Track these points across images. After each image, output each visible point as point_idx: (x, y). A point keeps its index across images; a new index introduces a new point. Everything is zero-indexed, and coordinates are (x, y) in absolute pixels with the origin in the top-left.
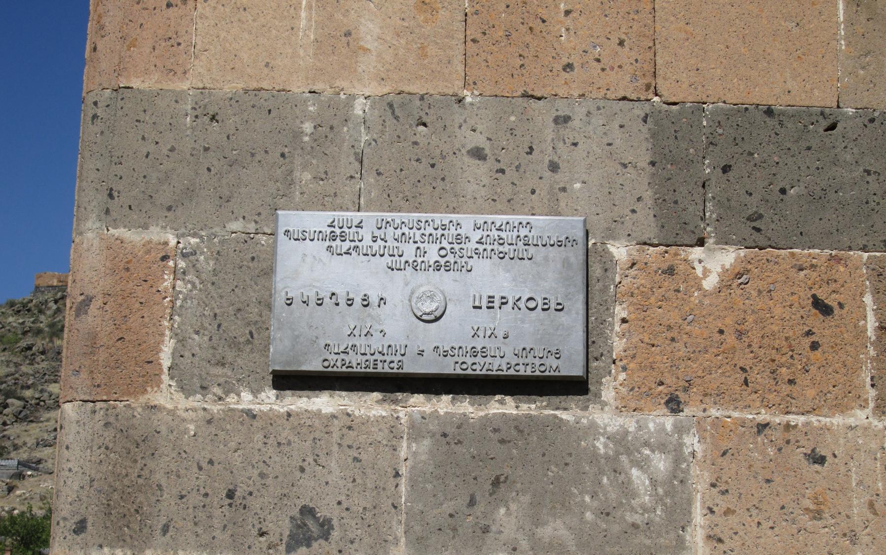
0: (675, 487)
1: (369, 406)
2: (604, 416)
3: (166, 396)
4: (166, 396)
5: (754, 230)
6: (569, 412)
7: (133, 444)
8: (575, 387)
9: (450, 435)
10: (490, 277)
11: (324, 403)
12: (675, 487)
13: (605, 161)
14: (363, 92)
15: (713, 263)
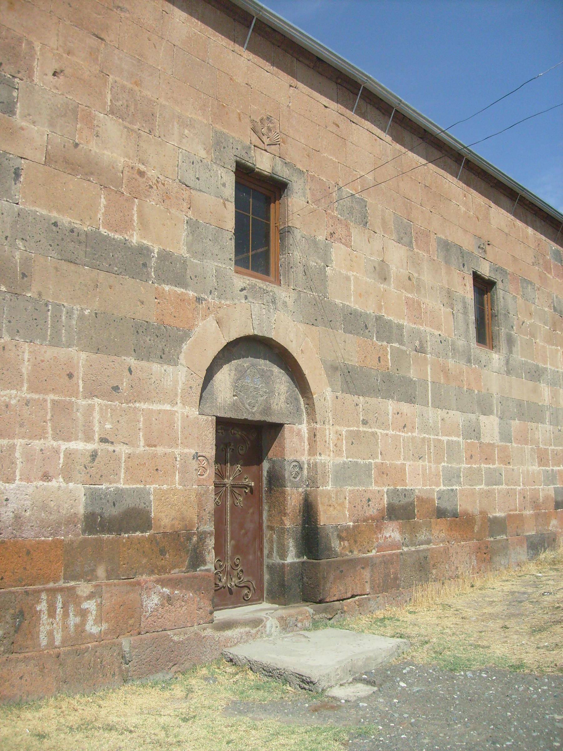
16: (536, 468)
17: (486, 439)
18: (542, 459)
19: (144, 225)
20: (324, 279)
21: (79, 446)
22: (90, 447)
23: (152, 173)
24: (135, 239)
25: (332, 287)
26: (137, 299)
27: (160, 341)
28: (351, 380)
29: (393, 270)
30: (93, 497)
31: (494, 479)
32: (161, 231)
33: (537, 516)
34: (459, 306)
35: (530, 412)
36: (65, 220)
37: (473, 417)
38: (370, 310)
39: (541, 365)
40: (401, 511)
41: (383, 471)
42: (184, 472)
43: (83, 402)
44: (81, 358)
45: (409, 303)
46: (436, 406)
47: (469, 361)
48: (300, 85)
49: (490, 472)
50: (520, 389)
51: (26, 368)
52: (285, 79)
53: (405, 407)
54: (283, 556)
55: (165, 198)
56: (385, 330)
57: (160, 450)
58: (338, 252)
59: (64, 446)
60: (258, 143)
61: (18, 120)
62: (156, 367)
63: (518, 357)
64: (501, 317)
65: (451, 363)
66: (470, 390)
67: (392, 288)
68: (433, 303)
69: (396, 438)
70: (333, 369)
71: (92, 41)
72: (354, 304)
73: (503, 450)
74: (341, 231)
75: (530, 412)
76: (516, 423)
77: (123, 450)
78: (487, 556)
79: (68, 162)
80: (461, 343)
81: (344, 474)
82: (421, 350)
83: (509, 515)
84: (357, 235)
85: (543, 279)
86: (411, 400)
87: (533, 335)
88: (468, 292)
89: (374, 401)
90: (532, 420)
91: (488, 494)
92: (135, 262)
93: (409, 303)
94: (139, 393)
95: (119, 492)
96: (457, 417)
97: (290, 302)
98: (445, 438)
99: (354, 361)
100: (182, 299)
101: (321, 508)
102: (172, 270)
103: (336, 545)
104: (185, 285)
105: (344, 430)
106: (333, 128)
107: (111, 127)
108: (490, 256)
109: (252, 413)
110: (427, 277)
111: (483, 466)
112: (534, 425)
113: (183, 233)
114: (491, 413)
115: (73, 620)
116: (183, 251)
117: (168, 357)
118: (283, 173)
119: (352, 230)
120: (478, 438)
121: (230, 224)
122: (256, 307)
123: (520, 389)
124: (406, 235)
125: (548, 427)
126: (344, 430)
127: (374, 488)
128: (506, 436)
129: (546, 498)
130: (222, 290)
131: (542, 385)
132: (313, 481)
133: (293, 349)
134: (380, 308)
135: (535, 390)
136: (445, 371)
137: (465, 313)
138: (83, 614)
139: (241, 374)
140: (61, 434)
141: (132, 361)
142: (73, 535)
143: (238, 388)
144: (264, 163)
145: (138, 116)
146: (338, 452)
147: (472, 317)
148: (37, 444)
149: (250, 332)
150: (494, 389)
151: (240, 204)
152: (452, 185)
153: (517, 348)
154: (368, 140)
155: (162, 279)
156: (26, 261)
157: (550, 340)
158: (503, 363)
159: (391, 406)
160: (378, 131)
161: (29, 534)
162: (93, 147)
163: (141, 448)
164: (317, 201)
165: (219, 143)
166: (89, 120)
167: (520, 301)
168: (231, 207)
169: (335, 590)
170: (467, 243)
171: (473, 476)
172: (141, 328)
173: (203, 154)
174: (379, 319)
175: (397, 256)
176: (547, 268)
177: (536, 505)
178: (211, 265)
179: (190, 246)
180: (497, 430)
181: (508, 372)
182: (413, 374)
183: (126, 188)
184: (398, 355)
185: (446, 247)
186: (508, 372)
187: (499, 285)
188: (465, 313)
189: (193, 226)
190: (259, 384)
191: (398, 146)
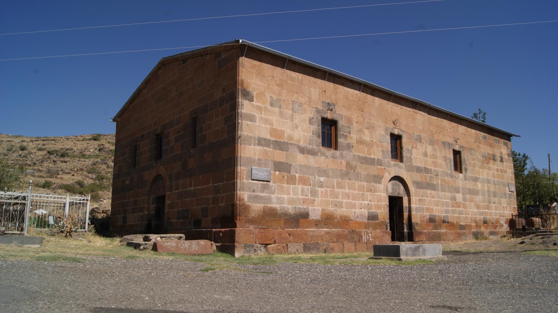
0: (275, 189)
1: (257, 182)
2: (271, 184)
3: (245, 180)
4: (245, 180)
5: (279, 171)
6: (269, 183)
7: (243, 184)
8: (269, 181)
9: (262, 184)
10: (265, 173)
11: (255, 182)
12: (275, 189)
13: (271, 164)
14: (257, 158)
15: (277, 173)
16: (476, 210)
17: (458, 201)
18: (478, 207)
19: (374, 153)
20: (411, 159)
21: (366, 202)
22: (368, 202)
23: (374, 140)
24: (372, 157)
25: (413, 161)
26: (373, 170)
27: (378, 179)
28: (419, 185)
29: (429, 153)
30: (369, 213)
31: (461, 213)
32: (377, 154)
33: (477, 226)
34: (448, 161)
35: (474, 192)
36: (361, 155)
37: (453, 194)
38: (422, 165)
39: (477, 176)
40: (432, 220)
41: (427, 209)
42: (384, 208)
43: (366, 193)
44: (365, 184)
45: (433, 162)
46: (442, 191)
47: (452, 177)
48: (403, 107)
49: (459, 211)
50: (470, 185)
51: (357, 187)
52: (400, 106)
53: (433, 192)
54: (403, 229)
55: (377, 145)
56: (427, 171)
57: (380, 203)
58: (414, 151)
59: (364, 202)
60: (394, 126)
61: (352, 135)
62: (378, 185)
63: (469, 174)
64: (463, 163)
65: (446, 178)
66: (452, 186)
67: (428, 159)
68: (440, 161)
69: (430, 200)
70: (415, 183)
71: (362, 113)
72: (419, 165)
73: (464, 204)
74: (415, 146)
75: (474, 192)
76: (468, 196)
77: (373, 203)
78: (459, 236)
79: (360, 142)
80: (449, 172)
81: (417, 210)
82: (437, 175)
83: (466, 225)
84: (419, 145)
85: (478, 147)
86: (434, 190)
87: (474, 167)
88: (451, 156)
89: (424, 190)
90: (474, 194)
91: (459, 217)
92: (372, 162)
93: (433, 162)
94: (375, 191)
95: (373, 212)
96: (448, 194)
97: (403, 166)
98: (445, 201)
99: (419, 180)
100: (382, 169)
101: (412, 218)
102: (380, 162)
103: (416, 227)
104: (381, 165)
105: (417, 198)
106: (411, 117)
107: (366, 131)
108: (458, 143)
109: (396, 194)
110: (438, 154)
111: (457, 209)
112: (475, 196)
113: (381, 153)
114: (459, 193)
115: (368, 237)
116: (381, 158)
117: (380, 183)
118: (401, 133)
119: (418, 145)
120: (455, 200)
121: (390, 149)
122: (396, 169)
123: (470, 185)
124: (432, 143)
125: (480, 197)
126: (417, 198)
127: (425, 213)
128: (465, 200)
129: (480, 220)
130: (389, 166)
131: (478, 183)
132: (410, 211)
133: (405, 178)
134: (425, 165)
135: (475, 185)
136: (444, 181)
137: (450, 163)
138: (369, 236)
139: (393, 185)
140: (363, 200)
141: (373, 184)
142: (366, 221)
143: (393, 189)
144: (396, 132)
145: (371, 128)
146: (416, 204)
147: (453, 164)
148: (360, 202)
149: (395, 175)
150: (460, 185)
151: (391, 143)
152: (446, 123)
153: (469, 171)
154: (421, 116)
155: (378, 165)
156: (356, 165)
157: (481, 167)
158: (463, 176)
159: (429, 191)
160: (423, 113)
161: (358, 220)
162: (364, 137)
163: (376, 203)
164: (408, 139)
165: (386, 129)
166: (363, 132)
167: (470, 156)
168: (390, 145)
169: (417, 239)
170: (451, 140)
171: (454, 212)
172: (375, 176)
173: (383, 133)
174: (425, 168)
175: (429, 149)
176: (480, 143)
177: (476, 222)
178: (387, 160)
179: (382, 156)
180: (461, 198)
181: (465, 180)
182: (435, 182)
183: (370, 145)
184: (431, 177)
185: (444, 143)
186: (465, 180)
187: (462, 152)
188: (450, 163)
189: (383, 151)
190: (397, 187)
191: (429, 116)
